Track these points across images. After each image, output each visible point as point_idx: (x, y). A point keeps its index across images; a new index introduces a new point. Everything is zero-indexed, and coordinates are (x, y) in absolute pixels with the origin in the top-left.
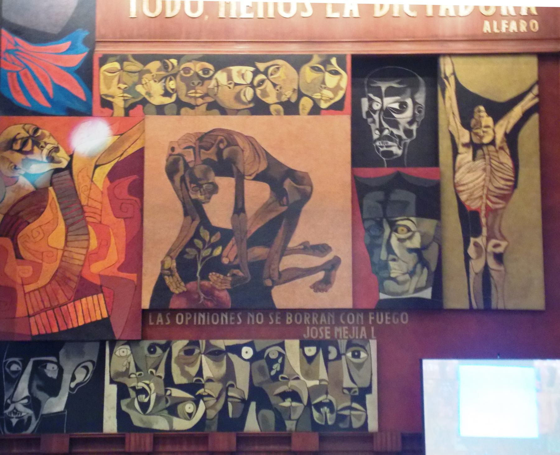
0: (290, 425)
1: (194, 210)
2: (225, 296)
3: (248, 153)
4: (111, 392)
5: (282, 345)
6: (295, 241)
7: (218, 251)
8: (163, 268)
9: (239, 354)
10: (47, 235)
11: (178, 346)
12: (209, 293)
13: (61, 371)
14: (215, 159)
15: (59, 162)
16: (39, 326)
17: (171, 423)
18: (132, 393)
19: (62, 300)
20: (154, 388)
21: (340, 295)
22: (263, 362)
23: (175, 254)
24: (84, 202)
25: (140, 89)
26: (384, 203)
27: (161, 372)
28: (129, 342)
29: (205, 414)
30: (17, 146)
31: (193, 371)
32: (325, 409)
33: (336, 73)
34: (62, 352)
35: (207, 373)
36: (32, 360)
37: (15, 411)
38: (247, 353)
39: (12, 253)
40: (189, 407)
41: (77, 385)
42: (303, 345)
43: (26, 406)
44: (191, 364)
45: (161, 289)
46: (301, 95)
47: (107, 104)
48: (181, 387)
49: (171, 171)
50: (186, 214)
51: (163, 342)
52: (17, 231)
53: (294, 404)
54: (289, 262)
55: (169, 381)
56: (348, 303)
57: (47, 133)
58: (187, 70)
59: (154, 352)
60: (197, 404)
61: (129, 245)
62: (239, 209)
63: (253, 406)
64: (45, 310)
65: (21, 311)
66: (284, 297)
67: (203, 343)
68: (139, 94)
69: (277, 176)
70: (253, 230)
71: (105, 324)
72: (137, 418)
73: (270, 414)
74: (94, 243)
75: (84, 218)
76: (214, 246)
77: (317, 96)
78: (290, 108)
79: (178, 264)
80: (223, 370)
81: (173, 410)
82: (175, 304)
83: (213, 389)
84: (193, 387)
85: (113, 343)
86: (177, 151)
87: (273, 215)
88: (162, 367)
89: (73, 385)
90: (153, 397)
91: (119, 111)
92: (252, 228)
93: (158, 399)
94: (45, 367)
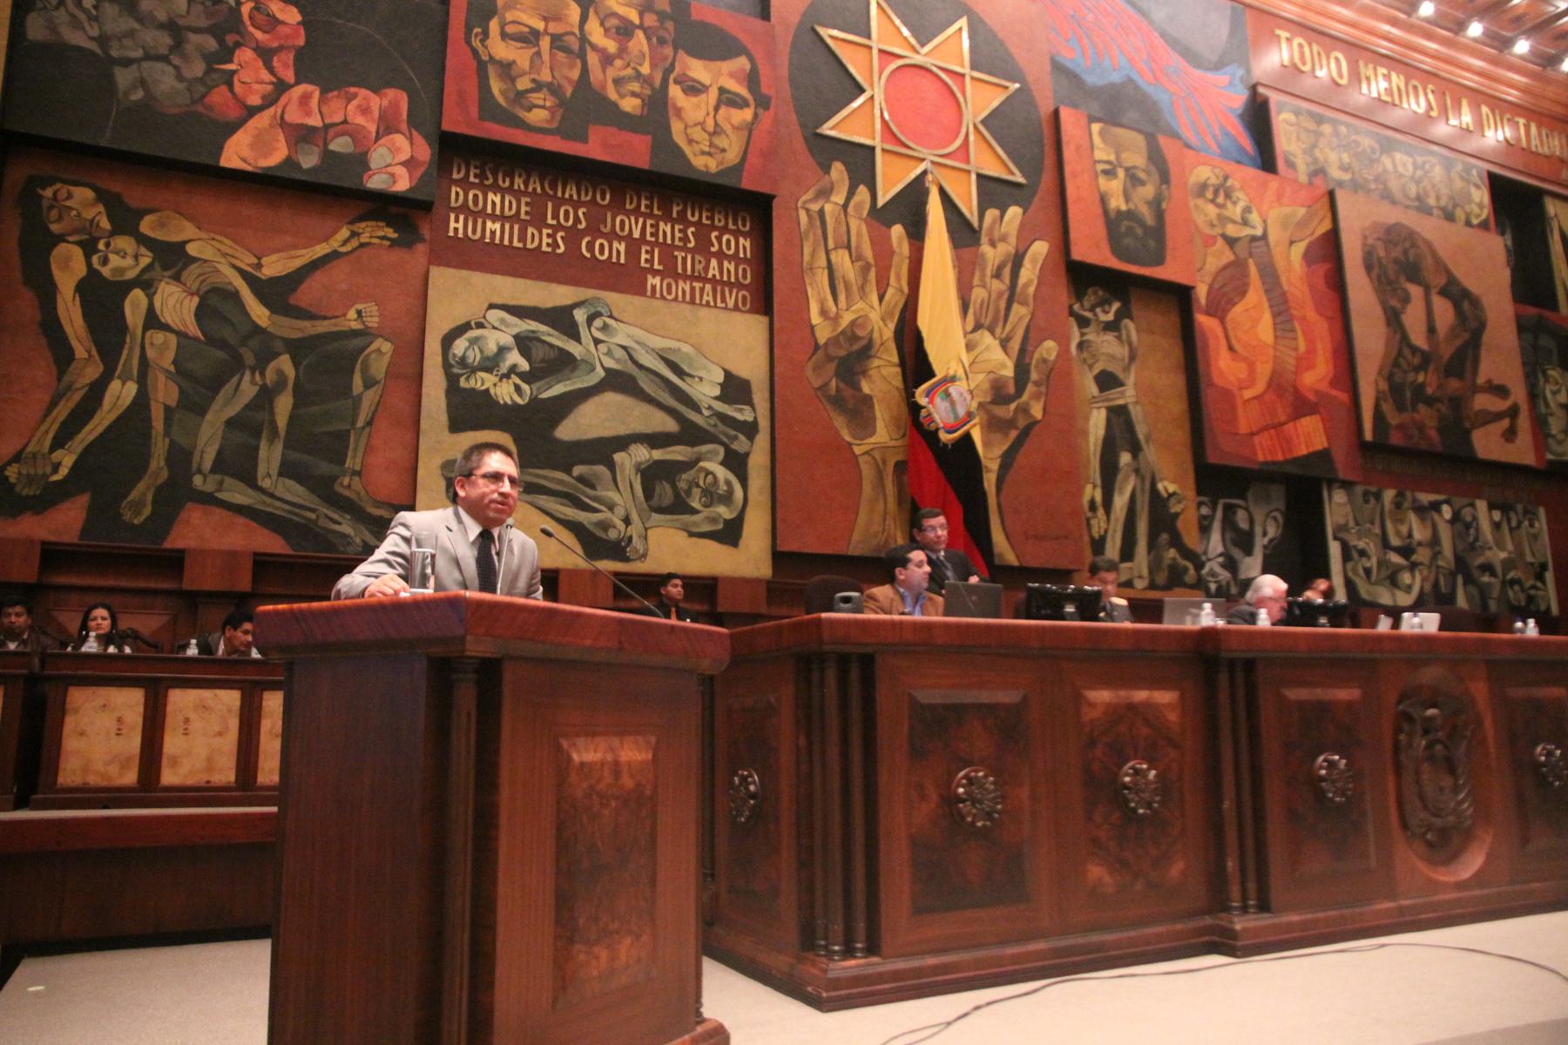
0: (1493, 606)
1: (1393, 318)
2: (1433, 433)
3: (1429, 260)
4: (1334, 549)
5: (1472, 505)
6: (1481, 380)
7: (1421, 378)
8: (1378, 392)
9: (1439, 511)
10: (1255, 322)
11: (1389, 495)
12: (1421, 428)
13: (1252, 522)
14: (1402, 258)
15: (1253, 227)
16: (1264, 451)
17: (1393, 595)
18: (1355, 555)
19: (1283, 418)
20: (1371, 546)
21: (1522, 452)
22: (1459, 526)
23: (1386, 372)
24: (1286, 288)
25: (1317, 153)
26: (1535, 347)
27: (1377, 530)
28: (1347, 485)
29: (1422, 588)
30: (1209, 195)
31: (1404, 529)
32: (1516, 588)
33: (1477, 186)
34: (1250, 495)
35: (1417, 536)
36: (1221, 502)
37: (1213, 574)
38: (1447, 512)
39: (1223, 342)
40: (1406, 578)
41: (1271, 541)
42: (1491, 507)
43: (1223, 566)
44: (1401, 521)
45: (1379, 417)
46: (1455, 206)
47: (1291, 165)
48: (1398, 550)
49: (1369, 268)
50: (1388, 324)
51: (1374, 489)
52: (1226, 311)
53: (1493, 580)
54: (1482, 402)
55: (1385, 544)
56: (1529, 459)
57: (1237, 185)
58: (1357, 143)
59: (1367, 502)
60: (1413, 577)
61: (1335, 352)
62: (1431, 330)
63: (1460, 580)
64: (1266, 428)
65: (1243, 428)
66: (1487, 444)
67: (1408, 494)
68: (1316, 161)
69: (1457, 294)
70: (1447, 356)
71: (1323, 456)
72: (1364, 591)
73: (1473, 590)
74: (1302, 345)
75: (1288, 309)
76: (1417, 369)
77: (1468, 209)
78: (1449, 217)
79: (1391, 388)
80: (1428, 534)
81: (1393, 581)
82: (1396, 439)
83: (1422, 555)
84: (1406, 551)
85: (1332, 482)
86: (1370, 241)
87: (1458, 343)
88: (1377, 522)
89: (1266, 541)
90: (1374, 560)
91: (1303, 178)
92: (1447, 352)
93: (1380, 563)
94: (1234, 513)
